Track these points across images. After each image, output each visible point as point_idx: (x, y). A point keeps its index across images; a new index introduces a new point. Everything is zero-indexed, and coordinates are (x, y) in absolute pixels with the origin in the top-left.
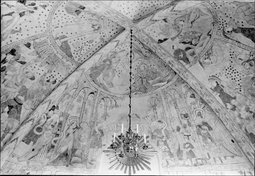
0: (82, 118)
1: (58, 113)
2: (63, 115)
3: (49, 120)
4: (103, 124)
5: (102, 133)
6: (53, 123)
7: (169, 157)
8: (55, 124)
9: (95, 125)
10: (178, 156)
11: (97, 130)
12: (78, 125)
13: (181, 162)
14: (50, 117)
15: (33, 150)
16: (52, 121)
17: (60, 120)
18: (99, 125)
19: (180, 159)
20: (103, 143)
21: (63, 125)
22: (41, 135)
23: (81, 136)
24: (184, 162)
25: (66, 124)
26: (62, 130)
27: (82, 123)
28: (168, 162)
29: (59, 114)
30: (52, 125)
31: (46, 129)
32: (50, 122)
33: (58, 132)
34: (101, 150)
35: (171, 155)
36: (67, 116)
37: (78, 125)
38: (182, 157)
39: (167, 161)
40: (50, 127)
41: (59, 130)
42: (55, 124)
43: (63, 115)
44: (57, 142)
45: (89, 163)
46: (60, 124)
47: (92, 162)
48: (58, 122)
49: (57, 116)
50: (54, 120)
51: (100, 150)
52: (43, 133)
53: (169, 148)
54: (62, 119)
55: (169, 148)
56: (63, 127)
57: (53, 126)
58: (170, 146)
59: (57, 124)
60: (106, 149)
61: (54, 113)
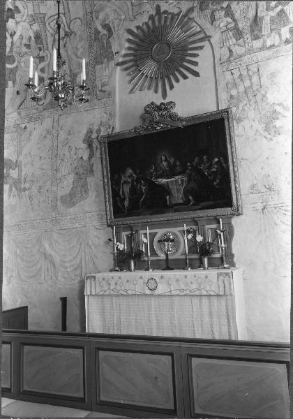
0: (69, 11)
1: (24, 18)
2: (34, 20)
3: (16, 37)
4: (108, 10)
5: (109, 30)
6: (24, 41)
7: (234, 40)
8: (30, 41)
9: (94, 19)
10: (252, 31)
11: (100, 28)
12: (67, 30)
13: (257, 44)
14: (15, 33)
15: (18, 93)
16: (21, 37)
17: (35, 31)
18: (101, 17)
19: (257, 38)
20: (115, 48)
21: (43, 37)
22: (17, 67)
23: (77, 49)
24: (265, 42)
25: (49, 35)
26: (45, 47)
27: (72, 23)
28: (231, 51)
29: (27, 21)
30: (25, 45)
31: (20, 55)
32: (19, 41)
33: (41, 53)
34: (113, 65)
35: (238, 34)
36: (43, 19)
37: (67, 30)
38: (261, 31)
39: (229, 48)
40: (24, 49)
41: (40, 50)
42: (30, 41)
43: (34, 20)
44: (46, 70)
45: (100, 91)
46: (38, 37)
47: (103, 89)
48: (32, 35)
49: (26, 25)
50: (24, 36)
51: (112, 64)
52: (19, 62)
53: (235, 21)
54: (36, 27)
55: (235, 21)
56: (44, 42)
57: (28, 46)
58: (237, 16)
59: (33, 38)
60: (121, 60)
61: (17, 23)
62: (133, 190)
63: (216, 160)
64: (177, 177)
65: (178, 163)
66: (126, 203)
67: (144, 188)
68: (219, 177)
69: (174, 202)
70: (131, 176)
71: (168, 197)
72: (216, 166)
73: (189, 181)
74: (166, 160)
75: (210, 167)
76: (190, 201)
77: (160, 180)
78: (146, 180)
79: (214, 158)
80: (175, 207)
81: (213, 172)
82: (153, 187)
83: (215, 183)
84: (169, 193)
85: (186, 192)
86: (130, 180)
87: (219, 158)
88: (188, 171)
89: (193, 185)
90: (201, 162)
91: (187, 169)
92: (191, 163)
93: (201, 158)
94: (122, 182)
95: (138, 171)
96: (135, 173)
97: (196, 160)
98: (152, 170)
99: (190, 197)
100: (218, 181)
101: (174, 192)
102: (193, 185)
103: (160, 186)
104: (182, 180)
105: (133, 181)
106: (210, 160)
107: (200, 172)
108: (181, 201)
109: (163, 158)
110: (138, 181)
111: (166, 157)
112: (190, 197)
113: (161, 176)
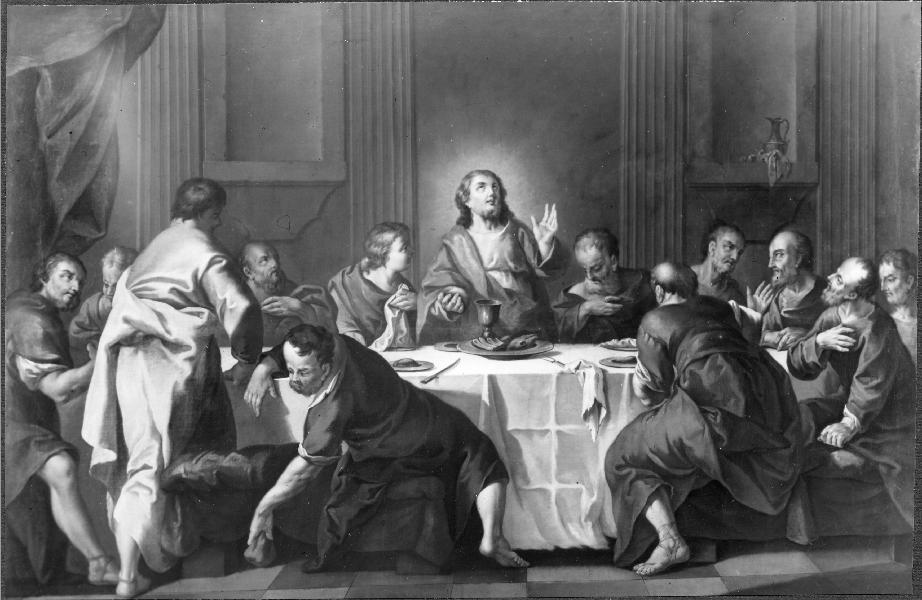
62: (205, 413)
63: (853, 272)
64: (571, 355)
65: (588, 252)
66: (134, 513)
67: (297, 408)
68: (861, 392)
69: (534, 540)
70: (199, 296)
71: (486, 499)
72: (848, 317)
73: (658, 393)
74: (500, 216)
75: (809, 314)
76: (642, 539)
77: (435, 356)
78: (320, 341)
79: (835, 264)
80: (537, 576)
81: (828, 354)
82: (369, 392)
83: (833, 434)
84: (498, 466)
85: (627, 471)
86: (183, 326)
87: (873, 268)
88: (654, 325)
89: (681, 423)
90: (753, 268)
91: (648, 304)
92: (682, 266)
93: (755, 244)
94: (112, 332)
95: (261, 264)
96: (236, 271)
97: (722, 249)
98: (380, 277)
99: (657, 515)
100: (850, 419)
101: (538, 458)
102: (681, 423)
103: (431, 406)
104: (606, 383)
105: (210, 343)
106: (813, 264)
107: (738, 343)
108: (585, 536)
109: (480, 199)
110: (255, 338)
111: (500, 193)
112: (657, 515)
113: (444, 332)
